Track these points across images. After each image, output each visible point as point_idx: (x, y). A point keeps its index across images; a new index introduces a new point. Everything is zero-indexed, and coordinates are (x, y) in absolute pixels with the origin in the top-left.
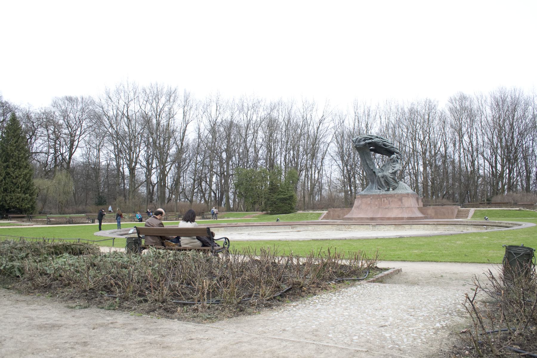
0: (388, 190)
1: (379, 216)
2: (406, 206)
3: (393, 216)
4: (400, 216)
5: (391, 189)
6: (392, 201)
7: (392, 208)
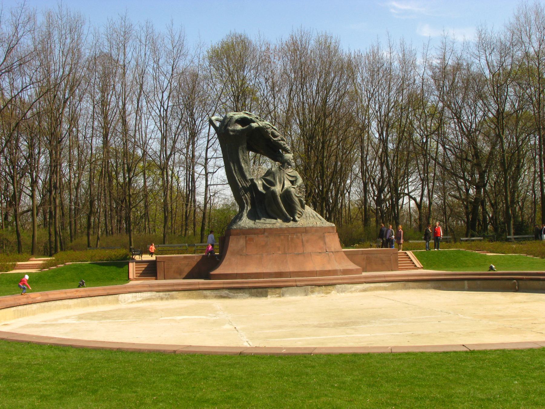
0: (294, 220)
1: (290, 268)
2: (333, 250)
3: (318, 269)
4: (329, 267)
5: (297, 219)
6: (307, 241)
7: (310, 254)
